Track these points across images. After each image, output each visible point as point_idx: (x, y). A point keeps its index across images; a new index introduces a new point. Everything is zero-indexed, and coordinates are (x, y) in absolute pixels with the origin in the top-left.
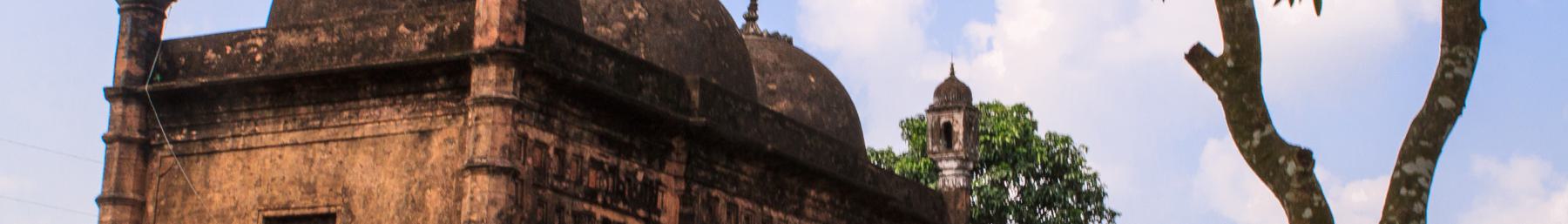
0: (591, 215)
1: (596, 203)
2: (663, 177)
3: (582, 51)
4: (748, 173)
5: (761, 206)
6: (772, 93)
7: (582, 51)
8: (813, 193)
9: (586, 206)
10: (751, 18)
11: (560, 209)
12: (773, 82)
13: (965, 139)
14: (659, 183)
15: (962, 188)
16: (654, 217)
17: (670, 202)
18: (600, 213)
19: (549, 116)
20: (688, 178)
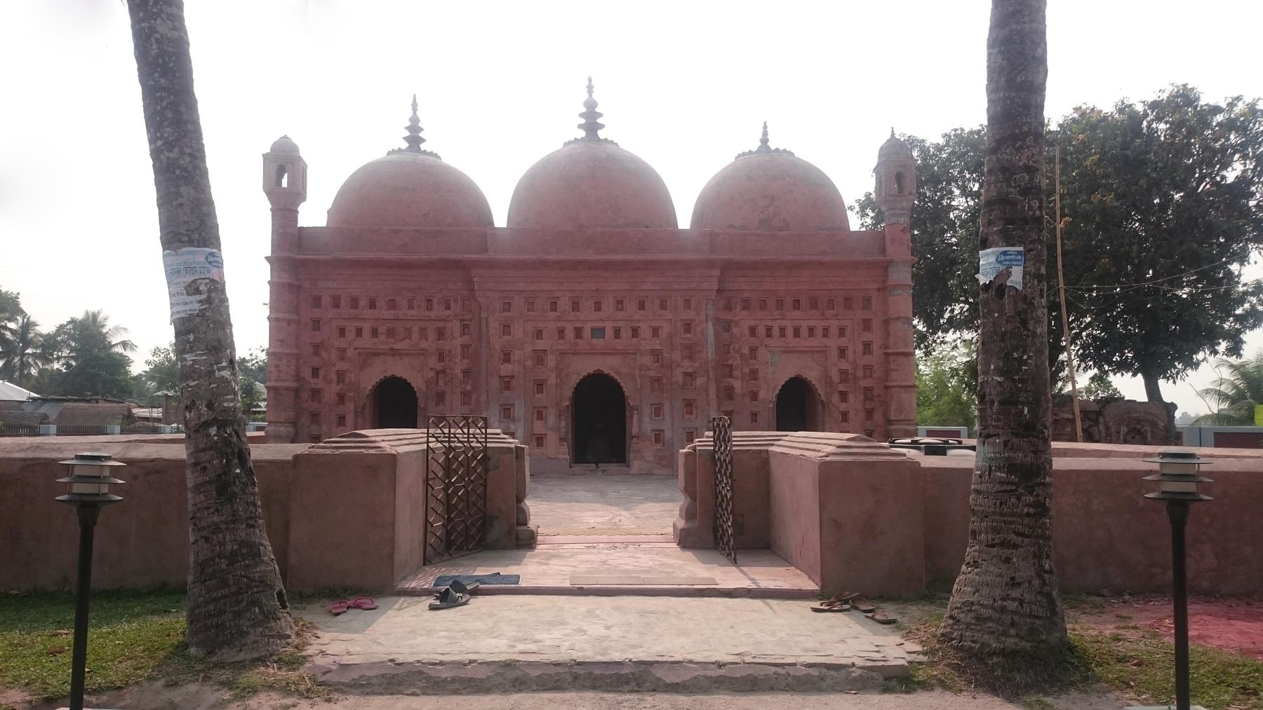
10: (764, 141)
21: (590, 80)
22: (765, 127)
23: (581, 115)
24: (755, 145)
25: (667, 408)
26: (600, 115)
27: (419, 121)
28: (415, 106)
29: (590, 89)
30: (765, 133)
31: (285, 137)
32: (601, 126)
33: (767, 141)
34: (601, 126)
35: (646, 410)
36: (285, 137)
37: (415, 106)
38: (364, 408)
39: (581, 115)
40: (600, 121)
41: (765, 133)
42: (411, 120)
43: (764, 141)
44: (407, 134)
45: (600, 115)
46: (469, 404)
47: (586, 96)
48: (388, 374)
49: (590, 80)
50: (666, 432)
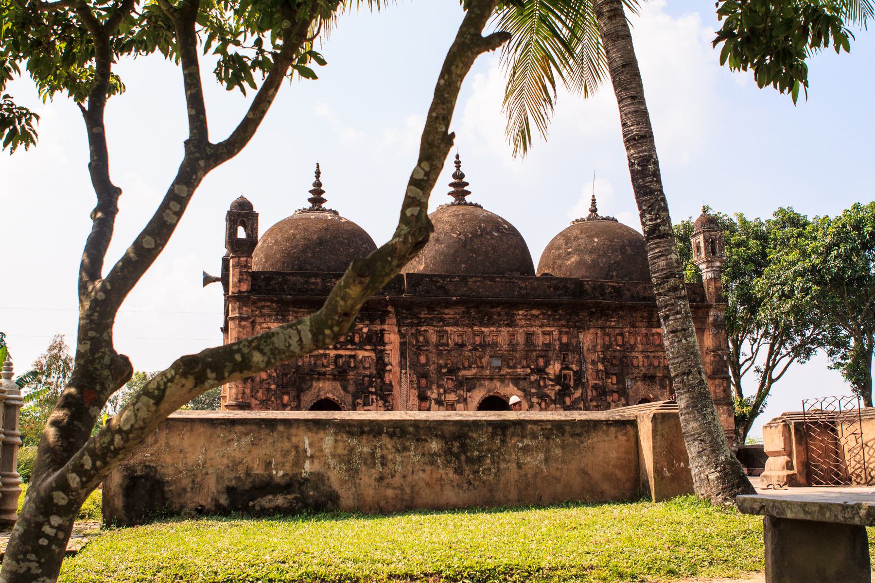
0: (325, 355)
1: (328, 349)
2: (386, 327)
3: (313, 280)
4: (450, 313)
5: (471, 327)
6: (569, 253)
7: (313, 280)
8: (521, 312)
9: (321, 352)
10: (594, 210)
12: (571, 247)
13: (706, 249)
14: (384, 330)
15: (711, 279)
17: (393, 339)
18: (332, 353)
19: (284, 316)
20: (399, 325)
22: (594, 200)
23: (451, 185)
24: (585, 214)
26: (467, 184)
28: (318, 173)
31: (242, 197)
32: (469, 193)
33: (596, 210)
34: (469, 193)
36: (242, 197)
37: (318, 173)
39: (451, 185)
40: (466, 188)
42: (314, 185)
43: (594, 210)
44: (311, 196)
45: (467, 184)
47: (455, 169)
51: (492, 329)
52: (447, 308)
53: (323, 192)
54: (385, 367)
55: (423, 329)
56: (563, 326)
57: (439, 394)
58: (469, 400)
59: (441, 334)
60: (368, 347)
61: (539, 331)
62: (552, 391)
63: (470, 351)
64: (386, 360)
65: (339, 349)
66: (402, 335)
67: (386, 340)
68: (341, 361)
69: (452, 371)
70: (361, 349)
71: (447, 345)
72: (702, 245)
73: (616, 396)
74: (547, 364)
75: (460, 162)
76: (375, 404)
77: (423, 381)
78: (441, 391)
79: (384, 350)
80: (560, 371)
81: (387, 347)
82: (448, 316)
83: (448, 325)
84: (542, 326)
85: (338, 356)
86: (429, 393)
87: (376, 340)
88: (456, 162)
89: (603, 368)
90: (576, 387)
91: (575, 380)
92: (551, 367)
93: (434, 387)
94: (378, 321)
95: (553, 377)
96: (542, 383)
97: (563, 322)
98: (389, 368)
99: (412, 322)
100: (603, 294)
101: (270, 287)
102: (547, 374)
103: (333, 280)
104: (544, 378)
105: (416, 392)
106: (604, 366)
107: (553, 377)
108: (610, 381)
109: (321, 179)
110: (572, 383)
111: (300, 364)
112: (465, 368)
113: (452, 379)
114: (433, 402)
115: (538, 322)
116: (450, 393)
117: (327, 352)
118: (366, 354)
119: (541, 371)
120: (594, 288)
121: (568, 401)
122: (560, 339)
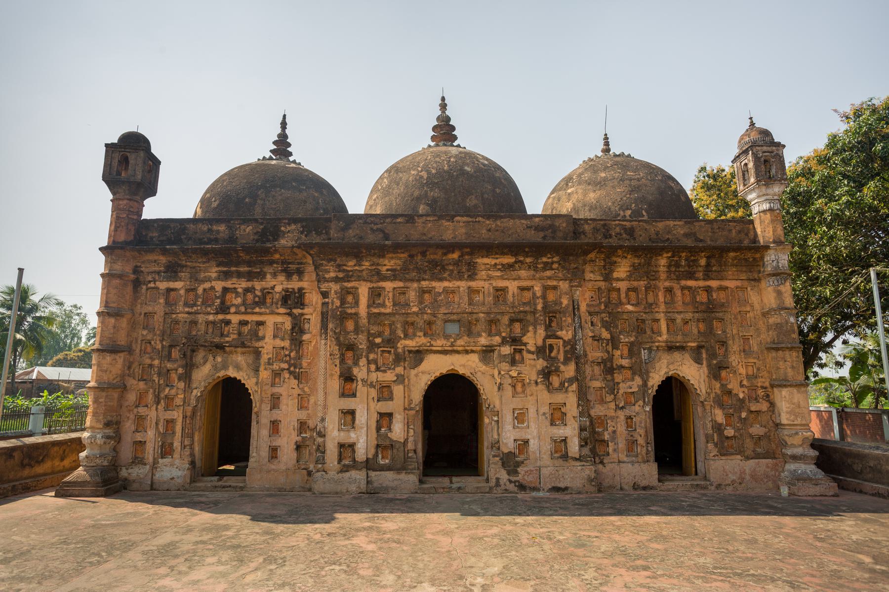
0: (228, 323)
1: (229, 313)
2: (304, 284)
4: (388, 264)
8: (486, 260)
9: (220, 317)
10: (607, 150)
11: (194, 323)
16: (296, 311)
17: (314, 298)
20: (320, 280)
21: (443, 99)
25: (532, 412)
27: (286, 137)
28: (284, 125)
29: (443, 106)
30: (607, 144)
35: (508, 418)
37: (284, 125)
38: (194, 413)
41: (607, 144)
42: (279, 136)
43: (607, 150)
46: (307, 408)
47: (440, 113)
48: (222, 374)
49: (443, 99)
50: (531, 442)
51: (446, 284)
52: (383, 256)
53: (289, 145)
54: (301, 336)
55: (349, 285)
56: (549, 278)
57: (369, 371)
58: (413, 379)
59: (375, 294)
60: (282, 310)
61: (512, 286)
62: (532, 367)
63: (416, 314)
64: (307, 326)
65: (246, 313)
66: (325, 295)
67: (307, 301)
68: (246, 329)
69: (391, 342)
70: (272, 313)
71: (383, 305)
72: (751, 165)
73: (629, 373)
74: (525, 332)
75: (446, 105)
76: (285, 385)
77: (349, 354)
78: (373, 367)
79: (303, 314)
80: (544, 341)
81: (306, 311)
82: (385, 268)
83: (385, 278)
84: (519, 278)
85: (243, 323)
86: (355, 371)
87: (293, 300)
88: (440, 105)
89: (609, 336)
90: (566, 361)
91: (566, 352)
92: (529, 334)
93: (363, 362)
94: (295, 277)
95: (533, 349)
96: (517, 357)
97: (548, 273)
98: (306, 337)
99: (337, 277)
100: (607, 236)
101: (164, 238)
102: (525, 344)
103: (243, 227)
104: (520, 351)
105: (337, 369)
106: (611, 334)
107: (533, 349)
108: (619, 352)
109: (287, 131)
110: (561, 357)
111: (194, 333)
112: (406, 336)
113: (389, 352)
114: (360, 383)
115: (514, 274)
116: (385, 371)
117: (228, 317)
118: (279, 319)
119: (515, 341)
120: (596, 230)
121: (555, 381)
122: (544, 297)
